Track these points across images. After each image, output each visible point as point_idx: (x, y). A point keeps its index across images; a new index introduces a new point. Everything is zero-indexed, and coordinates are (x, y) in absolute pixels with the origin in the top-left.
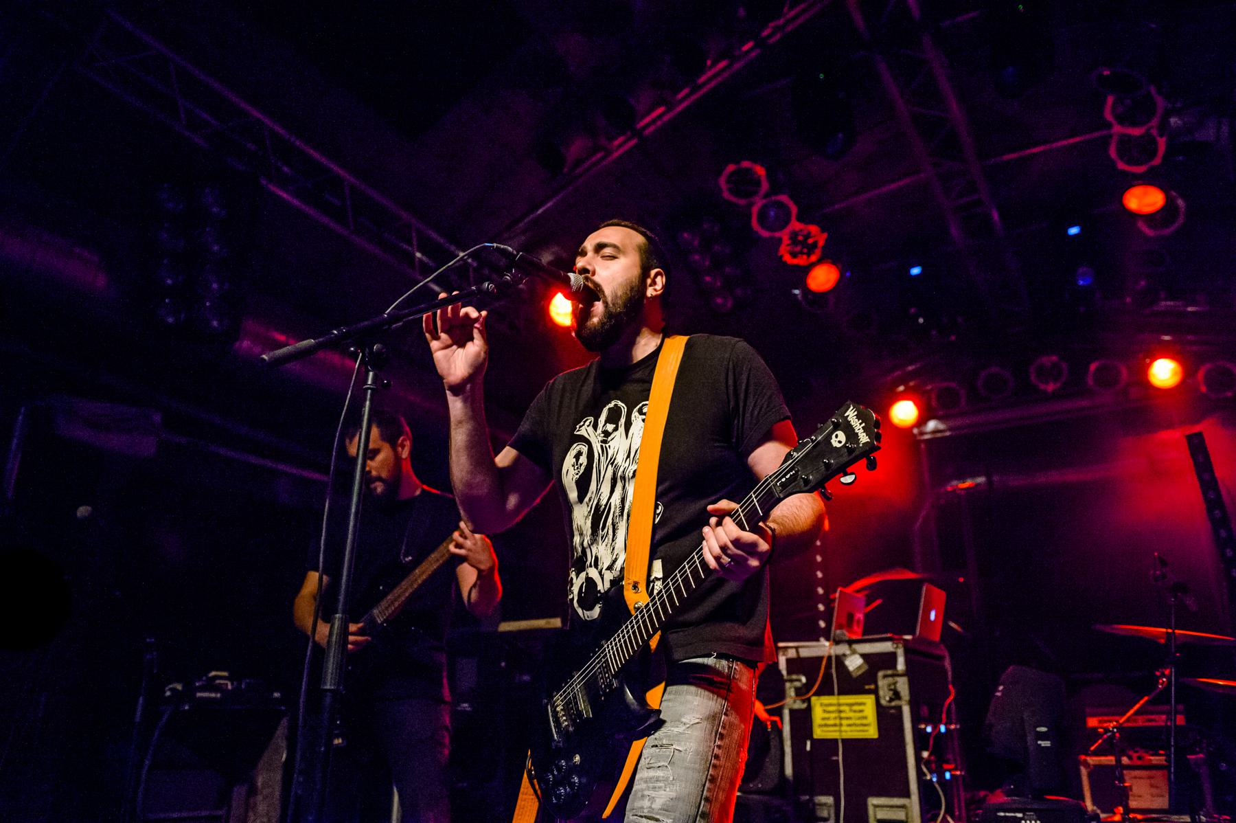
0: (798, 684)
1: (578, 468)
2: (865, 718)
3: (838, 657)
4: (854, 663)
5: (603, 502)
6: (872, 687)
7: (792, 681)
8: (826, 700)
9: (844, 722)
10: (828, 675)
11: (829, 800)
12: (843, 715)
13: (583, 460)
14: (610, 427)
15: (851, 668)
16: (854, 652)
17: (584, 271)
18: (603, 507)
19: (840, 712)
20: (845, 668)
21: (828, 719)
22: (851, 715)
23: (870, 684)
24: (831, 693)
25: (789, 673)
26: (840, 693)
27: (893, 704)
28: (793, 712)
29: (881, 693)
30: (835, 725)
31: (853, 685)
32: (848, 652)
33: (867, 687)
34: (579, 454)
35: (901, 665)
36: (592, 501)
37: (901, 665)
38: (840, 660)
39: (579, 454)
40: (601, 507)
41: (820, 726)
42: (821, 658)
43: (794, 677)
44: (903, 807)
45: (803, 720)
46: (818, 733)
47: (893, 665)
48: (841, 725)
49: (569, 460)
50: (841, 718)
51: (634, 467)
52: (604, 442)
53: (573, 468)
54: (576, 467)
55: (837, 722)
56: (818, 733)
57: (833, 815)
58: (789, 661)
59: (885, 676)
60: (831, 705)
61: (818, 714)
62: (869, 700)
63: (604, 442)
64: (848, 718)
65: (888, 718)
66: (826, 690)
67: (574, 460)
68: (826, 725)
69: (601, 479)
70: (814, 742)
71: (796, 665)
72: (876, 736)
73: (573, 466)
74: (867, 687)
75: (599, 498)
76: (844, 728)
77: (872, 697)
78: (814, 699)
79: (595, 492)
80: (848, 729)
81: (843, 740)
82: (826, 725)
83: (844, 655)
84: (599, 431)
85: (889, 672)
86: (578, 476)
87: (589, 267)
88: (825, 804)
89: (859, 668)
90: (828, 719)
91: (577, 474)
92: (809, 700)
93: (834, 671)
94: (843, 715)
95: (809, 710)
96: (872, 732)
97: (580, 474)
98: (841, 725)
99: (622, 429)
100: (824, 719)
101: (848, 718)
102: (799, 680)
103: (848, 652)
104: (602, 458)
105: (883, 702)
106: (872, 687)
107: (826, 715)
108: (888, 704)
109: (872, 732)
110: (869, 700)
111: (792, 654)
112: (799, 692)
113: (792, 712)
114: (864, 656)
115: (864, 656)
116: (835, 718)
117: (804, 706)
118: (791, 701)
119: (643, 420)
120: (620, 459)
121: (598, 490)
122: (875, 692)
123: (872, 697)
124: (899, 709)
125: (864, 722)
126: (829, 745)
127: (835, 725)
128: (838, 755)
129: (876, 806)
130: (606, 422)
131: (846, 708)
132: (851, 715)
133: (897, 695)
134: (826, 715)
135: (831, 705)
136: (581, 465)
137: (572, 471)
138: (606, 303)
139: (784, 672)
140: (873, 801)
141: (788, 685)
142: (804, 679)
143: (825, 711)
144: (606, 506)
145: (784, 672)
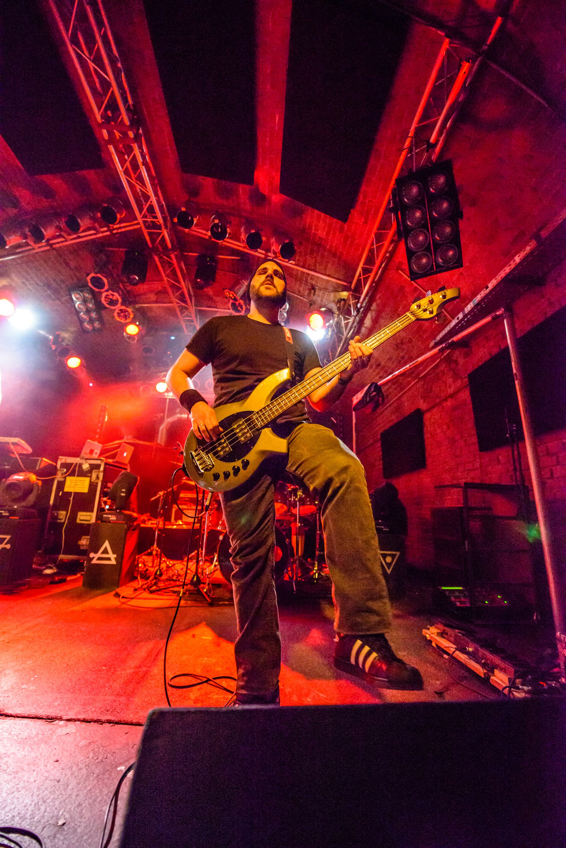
0: (63, 472)
7: (61, 470)
8: (72, 478)
12: (77, 484)
20: (82, 468)
23: (89, 474)
24: (74, 476)
25: (61, 467)
28: (59, 482)
31: (83, 474)
33: (88, 475)
35: (102, 468)
38: (80, 465)
44: (90, 515)
45: (61, 485)
46: (66, 489)
56: (66, 489)
57: (64, 518)
64: (79, 485)
65: (93, 486)
66: (72, 474)
71: (64, 465)
74: (88, 475)
85: (97, 471)
88: (62, 514)
92: (65, 477)
93: (77, 468)
95: (65, 481)
96: (86, 490)
101: (79, 485)
105: (92, 481)
106: (90, 475)
109: (86, 490)
111: (63, 461)
112: (62, 474)
117: (63, 480)
118: (59, 477)
122: (91, 477)
124: (97, 483)
133: (98, 478)
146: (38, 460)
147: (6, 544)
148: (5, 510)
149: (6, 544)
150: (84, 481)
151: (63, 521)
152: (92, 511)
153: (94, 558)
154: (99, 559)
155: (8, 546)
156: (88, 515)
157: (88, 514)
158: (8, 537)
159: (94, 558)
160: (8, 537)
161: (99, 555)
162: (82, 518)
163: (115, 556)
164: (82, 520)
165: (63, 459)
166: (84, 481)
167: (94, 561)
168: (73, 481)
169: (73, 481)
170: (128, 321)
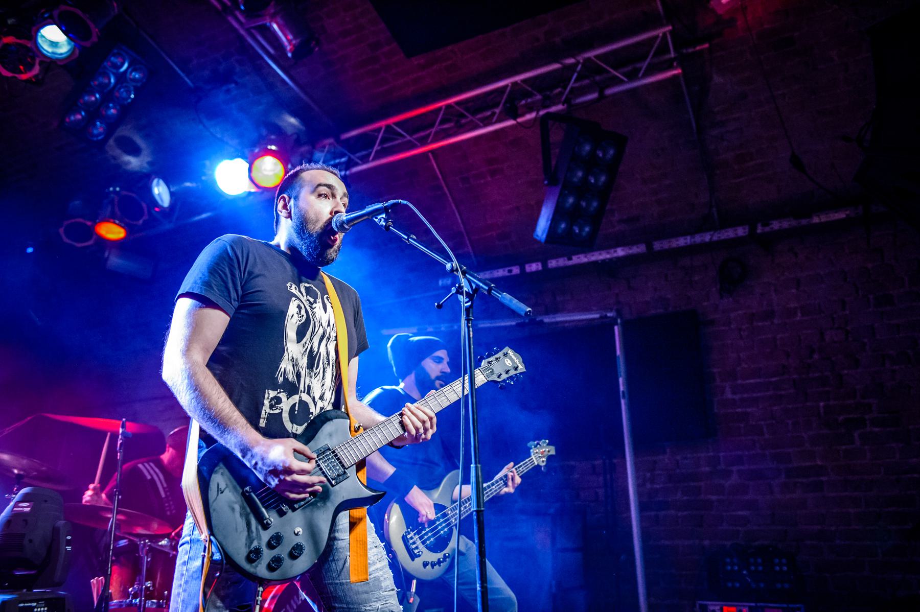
1: (301, 317)
5: (316, 349)
18: (315, 353)
36: (307, 345)
40: (314, 352)
53: (297, 315)
54: (299, 316)
67: (297, 310)
69: (315, 333)
73: (297, 313)
75: (312, 345)
79: (309, 339)
86: (300, 323)
91: (300, 321)
97: (302, 322)
119: (332, 307)
121: (311, 340)
136: (303, 316)
137: (296, 315)
144: (317, 353)
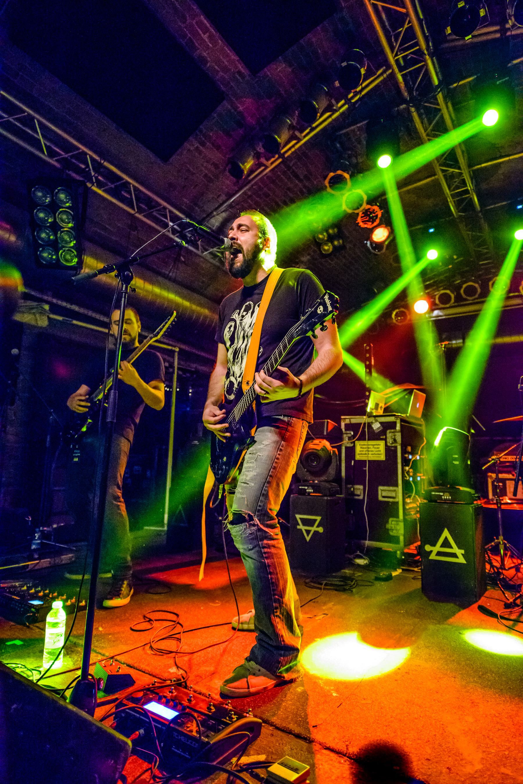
0: (350, 435)
2: (380, 451)
3: (368, 423)
4: (376, 426)
6: (384, 437)
7: (347, 434)
8: (362, 442)
9: (370, 453)
10: (363, 432)
11: (361, 487)
12: (369, 450)
13: (232, 329)
14: (245, 313)
15: (375, 429)
16: (376, 421)
17: (233, 239)
19: (368, 448)
20: (372, 428)
21: (363, 451)
22: (373, 449)
23: (383, 436)
24: (365, 440)
25: (346, 430)
26: (369, 440)
27: (393, 445)
28: (346, 448)
29: (388, 440)
30: (366, 454)
31: (375, 436)
32: (374, 421)
34: (231, 326)
35: (398, 427)
37: (398, 427)
38: (370, 425)
39: (231, 326)
41: (359, 454)
42: (361, 423)
43: (348, 432)
44: (395, 491)
45: (351, 451)
46: (358, 457)
47: (395, 427)
48: (368, 454)
49: (227, 329)
50: (368, 451)
51: (251, 331)
52: (241, 320)
55: (367, 453)
56: (358, 457)
57: (362, 492)
58: (346, 425)
59: (390, 432)
60: (364, 445)
61: (358, 449)
62: (382, 443)
63: (241, 320)
64: (372, 451)
65: (390, 452)
66: (362, 438)
68: (361, 454)
70: (355, 461)
71: (349, 427)
72: (384, 459)
74: (381, 437)
76: (369, 456)
77: (384, 441)
78: (356, 442)
80: (372, 456)
81: (369, 461)
82: (361, 454)
83: (372, 423)
84: (240, 316)
85: (393, 431)
87: (235, 237)
88: (359, 489)
89: (379, 428)
90: (363, 451)
92: (354, 442)
93: (366, 430)
94: (369, 450)
95: (354, 446)
96: (383, 458)
98: (368, 454)
99: (249, 314)
100: (361, 451)
101: (372, 451)
102: (351, 434)
103: (374, 421)
104: (240, 328)
105: (389, 444)
106: (384, 437)
107: (362, 450)
108: (391, 445)
109: (383, 458)
110: (382, 443)
111: (347, 421)
112: (349, 438)
113: (346, 448)
114: (381, 423)
115: (381, 423)
116: (366, 451)
117: (352, 445)
118: (346, 443)
120: (246, 328)
122: (385, 439)
123: (384, 441)
124: (396, 447)
125: (379, 453)
126: (363, 463)
127: (366, 454)
128: (366, 467)
129: (382, 490)
130: (244, 311)
131: (372, 447)
132: (373, 449)
133: (395, 441)
134: (362, 450)
135: (364, 445)
138: (244, 255)
139: (344, 430)
140: (380, 488)
141: (345, 436)
142: (352, 433)
143: (361, 448)
145: (344, 430)
146: (324, 422)
147: (318, 526)
148: (308, 486)
149: (318, 526)
150: (378, 445)
151: (361, 497)
152: (396, 485)
153: (431, 551)
154: (439, 554)
155: (321, 530)
156: (392, 491)
157: (391, 488)
158: (319, 518)
159: (431, 551)
160: (319, 518)
161: (437, 548)
162: (384, 494)
163: (463, 552)
164: (384, 497)
165: (346, 420)
166: (378, 445)
167: (433, 557)
168: (364, 447)
169: (364, 447)
170: (375, 224)
